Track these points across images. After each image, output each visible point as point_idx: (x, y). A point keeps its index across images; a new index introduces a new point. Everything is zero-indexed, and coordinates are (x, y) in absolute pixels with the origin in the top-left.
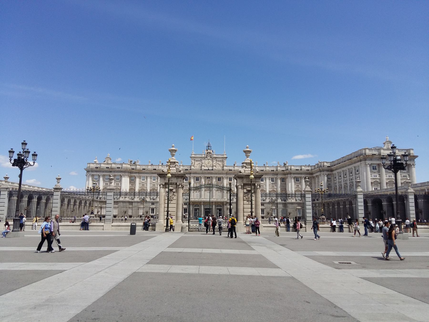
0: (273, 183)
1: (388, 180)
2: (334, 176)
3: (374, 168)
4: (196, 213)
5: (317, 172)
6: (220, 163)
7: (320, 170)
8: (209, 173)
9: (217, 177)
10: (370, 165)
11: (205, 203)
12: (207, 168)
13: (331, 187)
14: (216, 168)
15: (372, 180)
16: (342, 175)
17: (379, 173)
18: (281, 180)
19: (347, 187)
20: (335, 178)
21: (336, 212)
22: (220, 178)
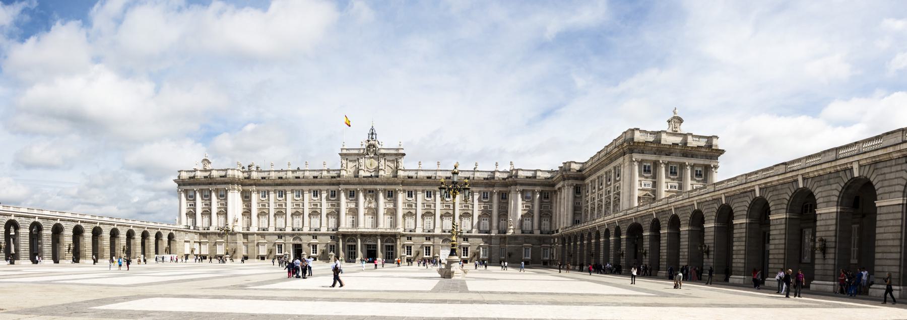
0: (487, 201)
1: (668, 193)
2: (585, 189)
3: (646, 170)
4: (352, 252)
5: (559, 182)
6: (392, 165)
7: (563, 176)
8: (371, 183)
9: (385, 190)
10: (640, 163)
11: (363, 236)
12: (368, 174)
13: (581, 208)
14: (385, 173)
15: (641, 192)
16: (597, 186)
17: (654, 180)
18: (501, 197)
19: (602, 208)
20: (588, 192)
21: (578, 252)
22: (392, 192)
